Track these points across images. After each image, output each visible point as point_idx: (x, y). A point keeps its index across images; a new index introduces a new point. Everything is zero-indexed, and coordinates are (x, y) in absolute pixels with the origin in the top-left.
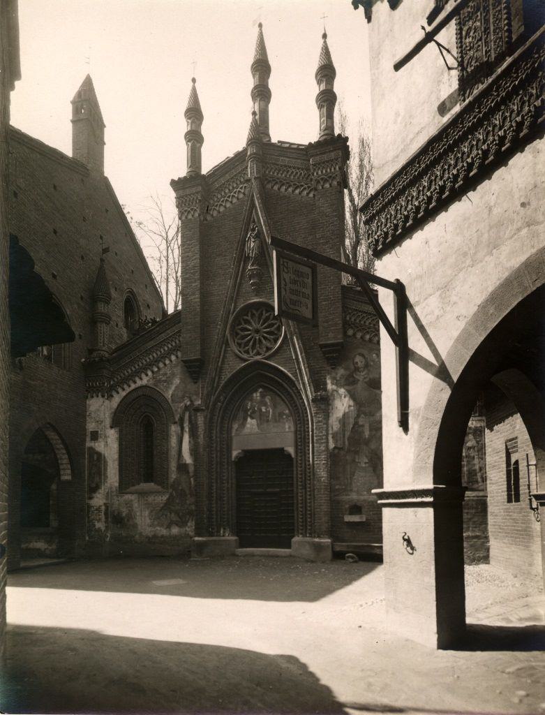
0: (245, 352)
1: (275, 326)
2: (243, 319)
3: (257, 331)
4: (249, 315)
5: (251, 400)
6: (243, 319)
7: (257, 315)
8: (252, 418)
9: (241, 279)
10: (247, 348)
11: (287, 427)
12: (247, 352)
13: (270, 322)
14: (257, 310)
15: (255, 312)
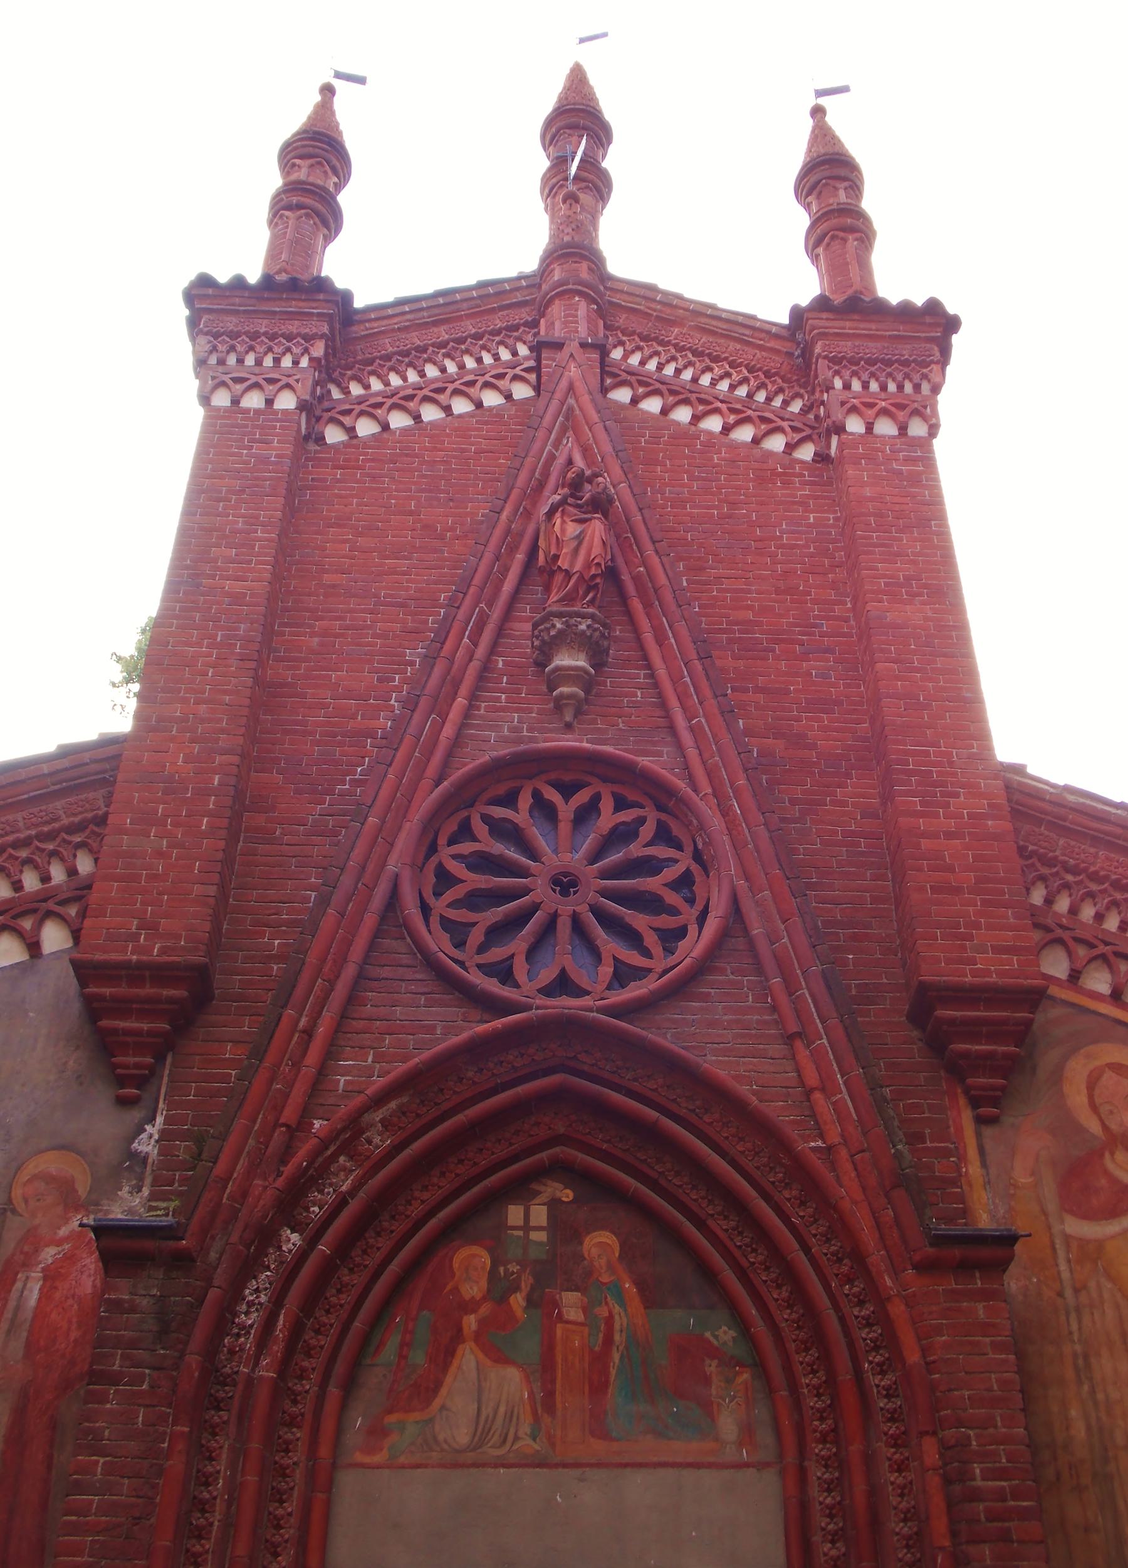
0: (487, 969)
1: (671, 873)
2: (486, 819)
3: (565, 883)
4: (525, 801)
5: (496, 1243)
6: (486, 819)
7: (566, 810)
8: (501, 1358)
9: (493, 651)
10: (496, 954)
11: (728, 1425)
12: (504, 973)
13: (635, 850)
14: (568, 790)
15: (552, 795)
